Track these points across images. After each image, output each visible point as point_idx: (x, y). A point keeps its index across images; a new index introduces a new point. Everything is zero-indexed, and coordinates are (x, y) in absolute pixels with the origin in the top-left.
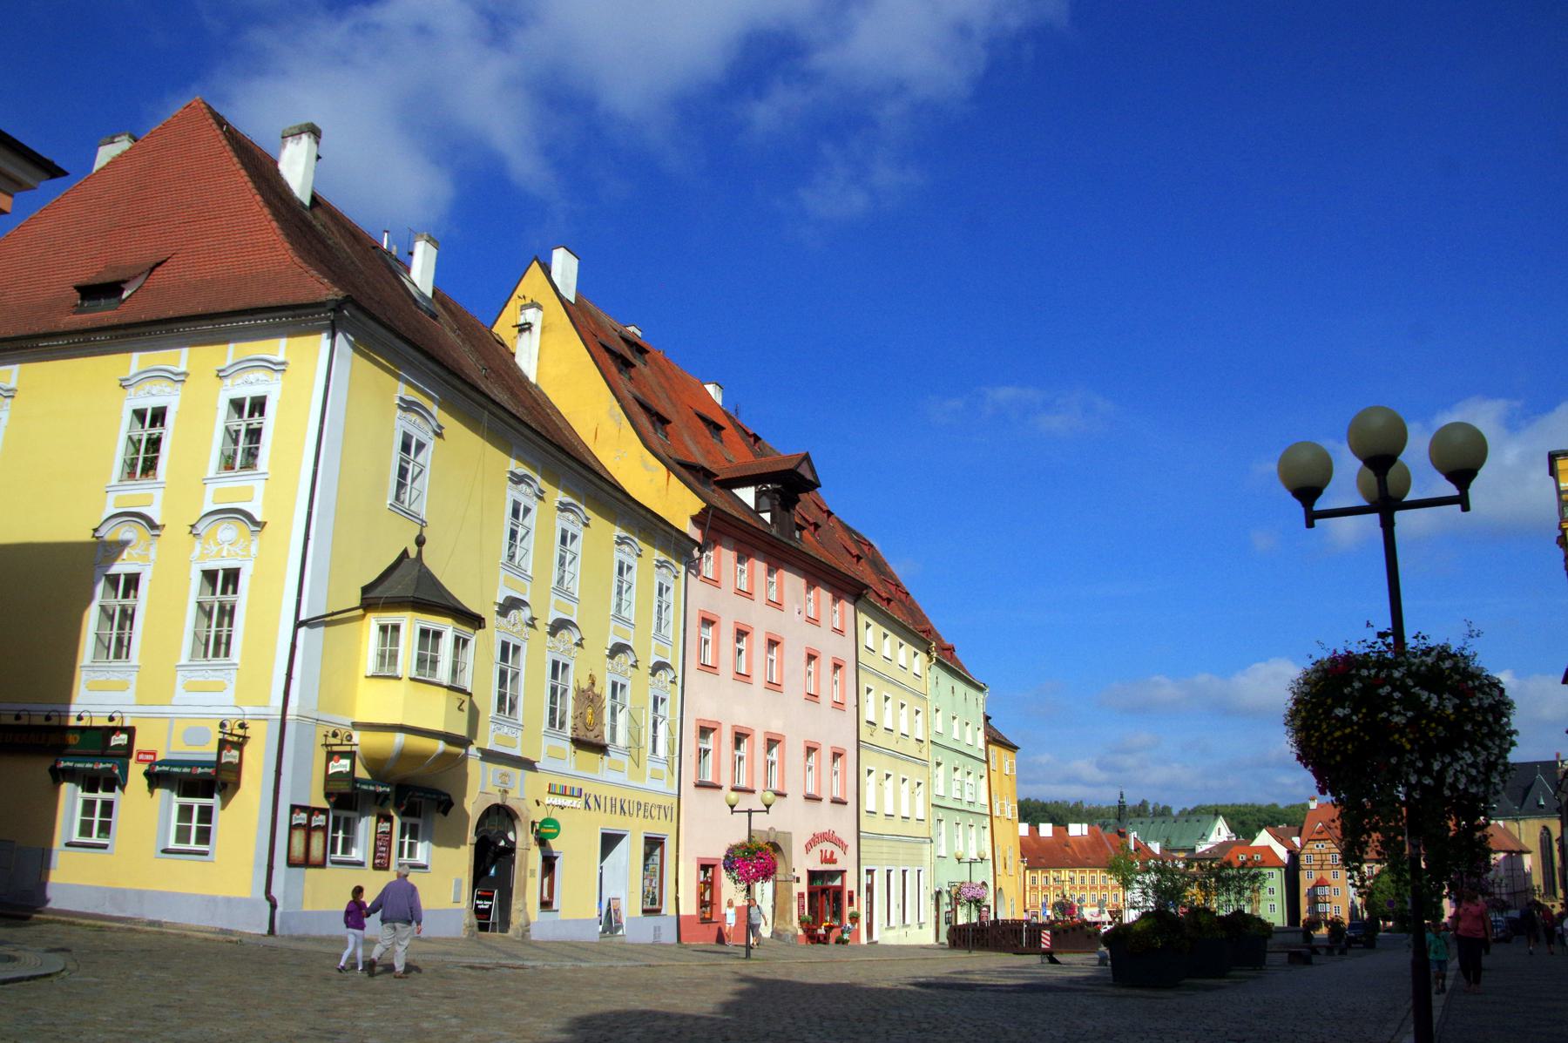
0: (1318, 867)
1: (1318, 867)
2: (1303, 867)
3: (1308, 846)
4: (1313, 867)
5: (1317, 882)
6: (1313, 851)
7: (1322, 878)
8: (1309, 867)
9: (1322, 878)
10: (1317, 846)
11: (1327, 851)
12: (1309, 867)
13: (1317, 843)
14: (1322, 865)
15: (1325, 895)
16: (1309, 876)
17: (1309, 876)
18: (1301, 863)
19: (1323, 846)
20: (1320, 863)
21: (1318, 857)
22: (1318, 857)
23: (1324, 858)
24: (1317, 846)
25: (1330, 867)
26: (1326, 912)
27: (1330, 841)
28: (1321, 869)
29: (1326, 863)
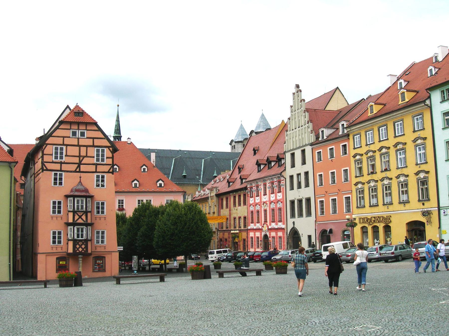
2: (49, 166)
3: (59, 133)
4: (65, 167)
5: (72, 191)
6: (67, 141)
8: (57, 167)
10: (74, 134)
11: (90, 142)
12: (57, 167)
14: (79, 164)
15: (86, 213)
16: (58, 181)
17: (58, 181)
18: (46, 158)
19: (83, 134)
20: (77, 160)
21: (74, 151)
22: (74, 151)
23: (83, 153)
24: (74, 134)
25: (93, 168)
28: (78, 171)
29: (85, 161)
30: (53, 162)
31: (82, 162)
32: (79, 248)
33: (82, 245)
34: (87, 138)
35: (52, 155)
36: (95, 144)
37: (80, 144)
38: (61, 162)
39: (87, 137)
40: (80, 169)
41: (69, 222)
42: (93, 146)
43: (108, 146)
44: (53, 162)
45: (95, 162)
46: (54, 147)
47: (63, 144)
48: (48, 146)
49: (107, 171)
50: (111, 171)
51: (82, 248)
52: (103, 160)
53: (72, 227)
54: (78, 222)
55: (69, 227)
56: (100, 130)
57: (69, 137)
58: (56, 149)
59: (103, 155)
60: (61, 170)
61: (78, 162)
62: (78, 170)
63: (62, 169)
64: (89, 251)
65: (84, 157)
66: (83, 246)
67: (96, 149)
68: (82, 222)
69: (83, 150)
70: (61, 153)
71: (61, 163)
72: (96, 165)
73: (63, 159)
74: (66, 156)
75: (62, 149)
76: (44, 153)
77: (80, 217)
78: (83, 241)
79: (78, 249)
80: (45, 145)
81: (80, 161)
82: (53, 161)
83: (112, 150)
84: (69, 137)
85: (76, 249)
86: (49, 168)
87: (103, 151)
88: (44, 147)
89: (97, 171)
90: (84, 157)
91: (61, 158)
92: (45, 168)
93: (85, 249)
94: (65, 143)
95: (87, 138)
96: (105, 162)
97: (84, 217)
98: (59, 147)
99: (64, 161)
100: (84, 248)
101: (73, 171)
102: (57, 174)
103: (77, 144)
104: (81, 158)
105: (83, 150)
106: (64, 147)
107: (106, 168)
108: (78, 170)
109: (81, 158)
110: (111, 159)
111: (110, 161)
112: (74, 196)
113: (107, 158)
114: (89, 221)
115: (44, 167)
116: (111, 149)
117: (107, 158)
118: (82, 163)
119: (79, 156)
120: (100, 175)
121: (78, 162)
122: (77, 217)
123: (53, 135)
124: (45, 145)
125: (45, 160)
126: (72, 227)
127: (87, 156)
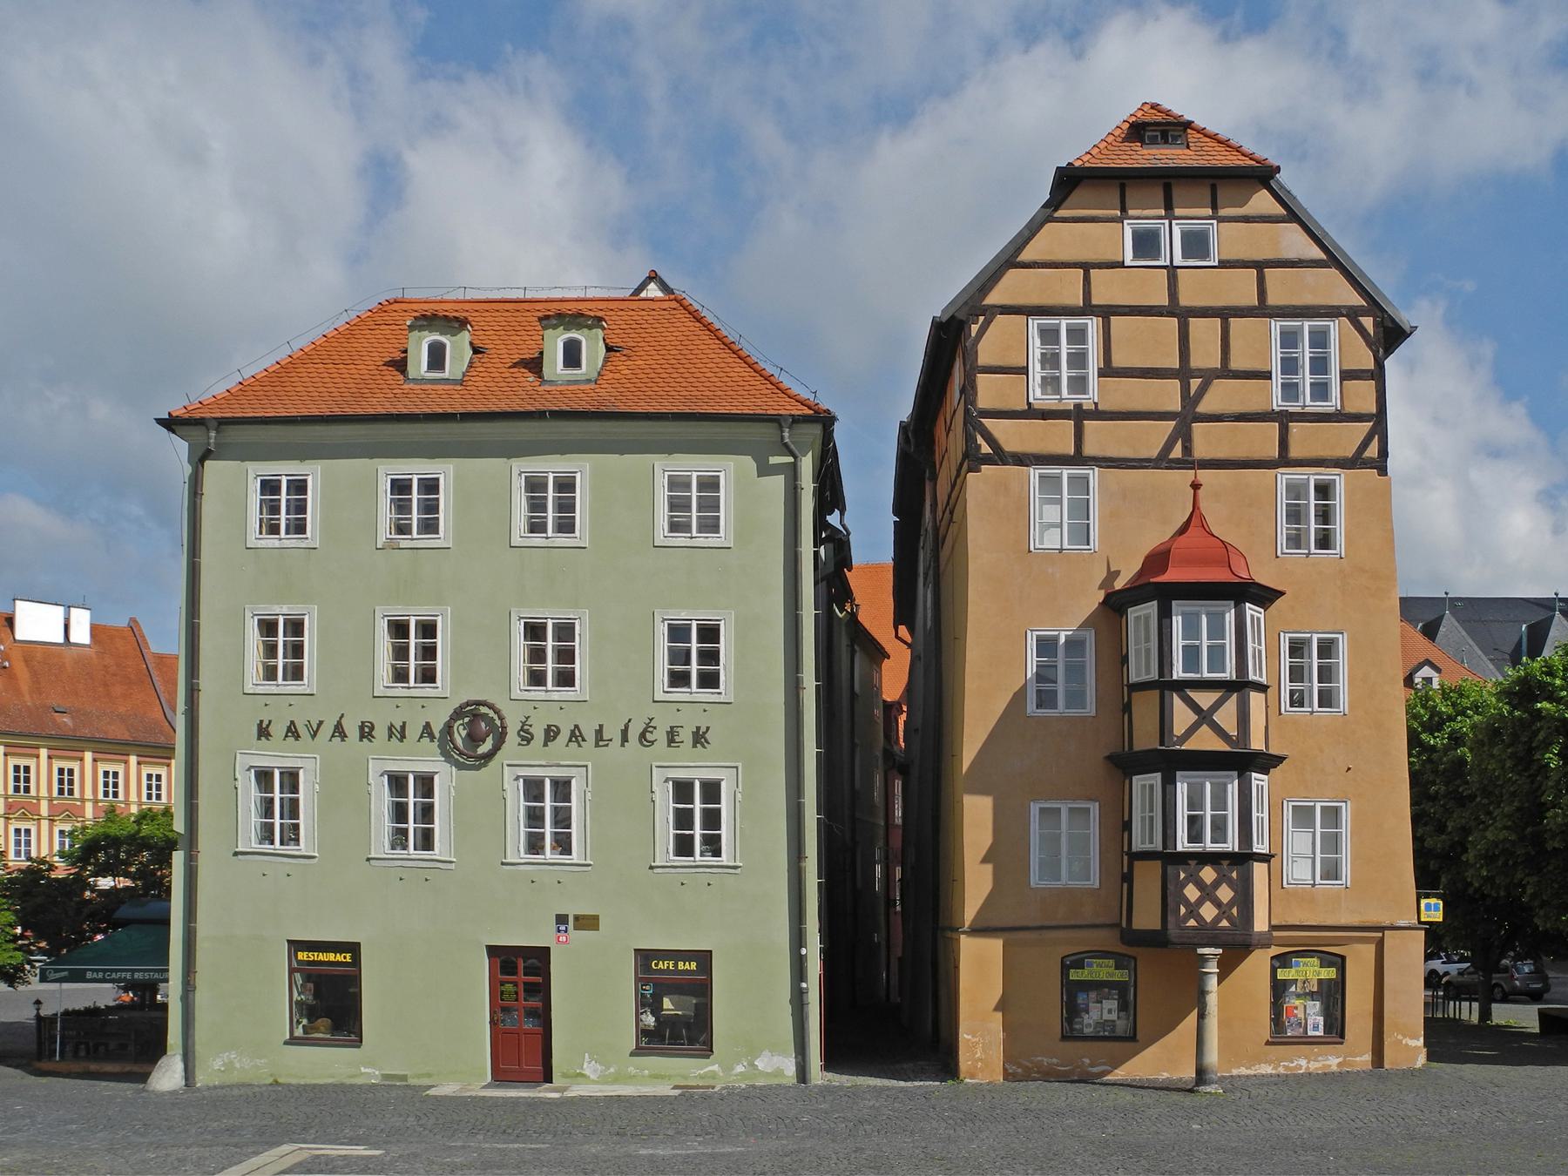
0: (1151, 439)
1: (1151, 439)
2: (1010, 435)
4: (1099, 439)
6: (1107, 288)
7: (1195, 519)
8: (1059, 437)
9: (1195, 519)
12: (1059, 437)
13: (1146, 216)
14: (1187, 418)
18: (989, 392)
19: (1196, 244)
20: (1168, 395)
23: (1205, 354)
24: (1146, 244)
25: (1264, 439)
26: (1244, 859)
27: (1262, 202)
29: (1220, 397)
30: (1031, 413)
31: (1202, 408)
32: (1200, 902)
33: (1216, 884)
34: (1224, 264)
35: (1024, 371)
36: (1273, 300)
37: (1185, 300)
38: (1078, 406)
39: (1224, 257)
40: (1187, 449)
41: (1139, 745)
42: (1263, 310)
43: (1351, 308)
44: (1031, 413)
45: (1277, 403)
46: (1034, 323)
47: (1088, 309)
48: (1000, 319)
49: (1349, 452)
50: (1372, 451)
51: (1217, 903)
52: (1321, 391)
53: (1159, 775)
54: (1190, 745)
55: (1135, 778)
56: (1293, 215)
57: (1121, 265)
58: (1049, 336)
59: (1320, 365)
60: (1078, 459)
61: (1176, 406)
62: (1177, 452)
63: (1089, 449)
64: (1260, 924)
65: (1209, 376)
66: (1225, 893)
67: (1276, 326)
68: (1220, 746)
69: (1205, 332)
70: (1078, 360)
71: (1079, 415)
72: (1284, 419)
73: (1085, 391)
74: (1107, 371)
75: (1077, 335)
76: (984, 359)
77: (1204, 717)
78: (1225, 863)
79: (1193, 910)
80: (981, 318)
81: (1189, 401)
82: (1029, 404)
83: (1371, 330)
84: (1121, 265)
85: (1183, 910)
86: (1009, 446)
87: (1320, 340)
88: (975, 328)
89: (1295, 452)
90: (1209, 376)
91: (1079, 384)
92: (986, 449)
93: (1235, 911)
94: (1095, 302)
95: (1224, 264)
96: (1333, 404)
97: (1226, 716)
98: (1064, 323)
99: (1096, 404)
100: (1231, 903)
101: (1148, 460)
102: (1059, 478)
103: (1164, 300)
104: (1195, 383)
105: (1205, 332)
106: (1093, 325)
107: (1348, 438)
108: (1177, 452)
109: (1195, 383)
110: (1369, 386)
111: (1362, 397)
112: (1168, 595)
113: (1346, 375)
114: (1257, 744)
115: (980, 440)
116: (1368, 322)
117: (1346, 375)
118: (1202, 408)
119: (1183, 373)
120: (1312, 476)
121: (1176, 406)
122: (1182, 717)
123: (1025, 256)
124: (981, 318)
125: (984, 401)
126: (1159, 775)
127: (1226, 372)
